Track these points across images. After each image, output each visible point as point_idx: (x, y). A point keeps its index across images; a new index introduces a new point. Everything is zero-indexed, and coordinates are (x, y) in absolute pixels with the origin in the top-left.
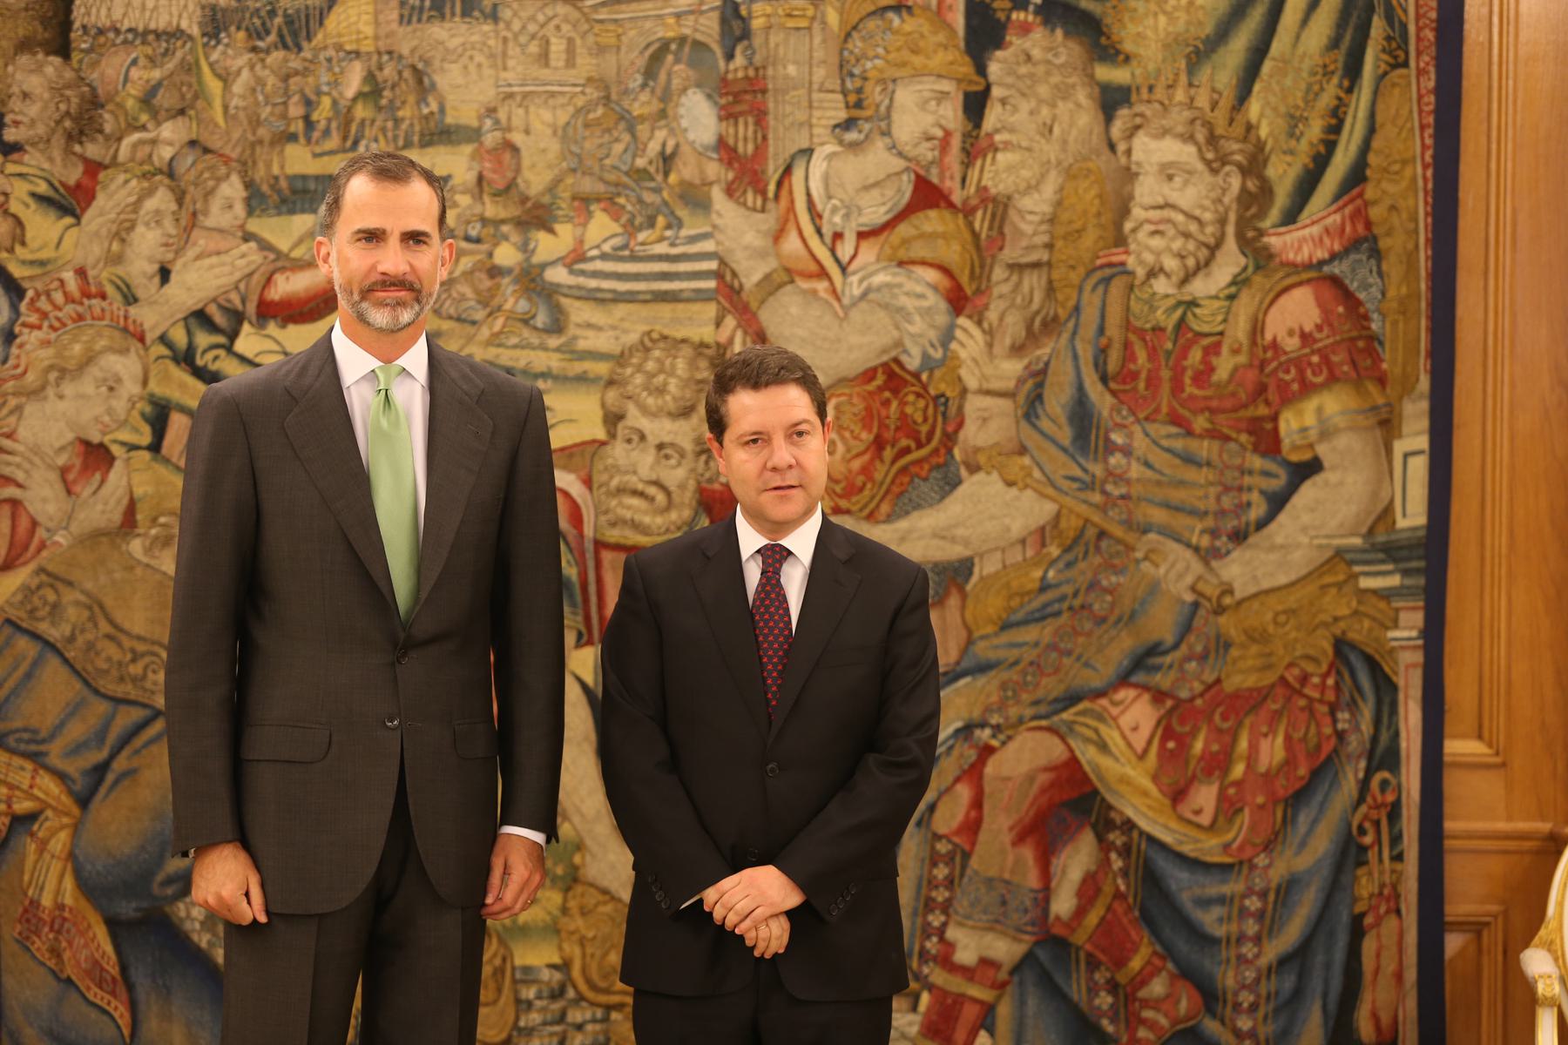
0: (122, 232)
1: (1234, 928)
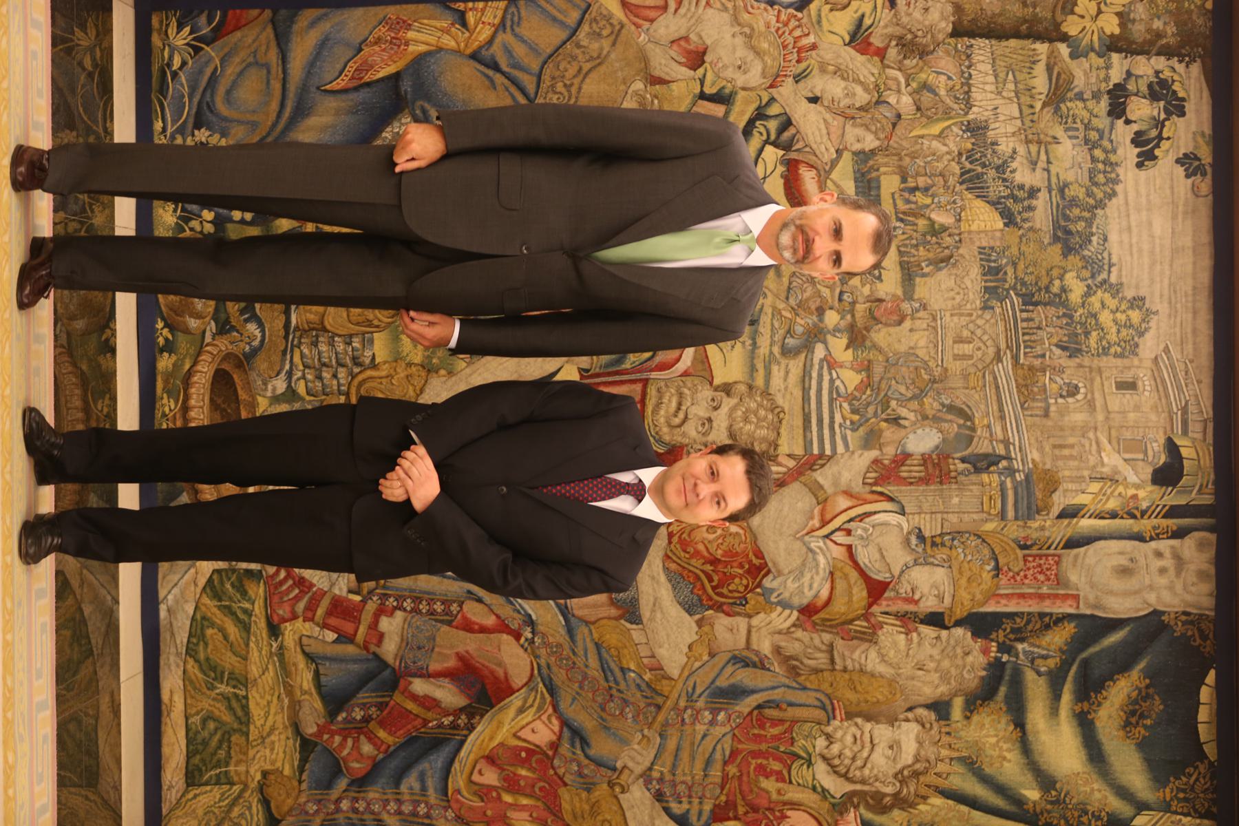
0: (840, 72)
1: (406, 797)
